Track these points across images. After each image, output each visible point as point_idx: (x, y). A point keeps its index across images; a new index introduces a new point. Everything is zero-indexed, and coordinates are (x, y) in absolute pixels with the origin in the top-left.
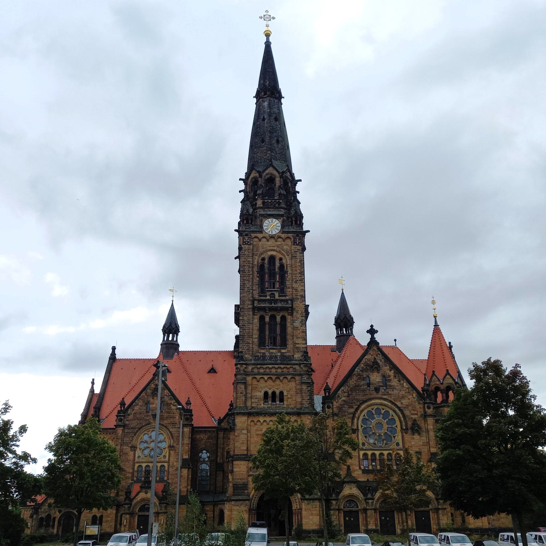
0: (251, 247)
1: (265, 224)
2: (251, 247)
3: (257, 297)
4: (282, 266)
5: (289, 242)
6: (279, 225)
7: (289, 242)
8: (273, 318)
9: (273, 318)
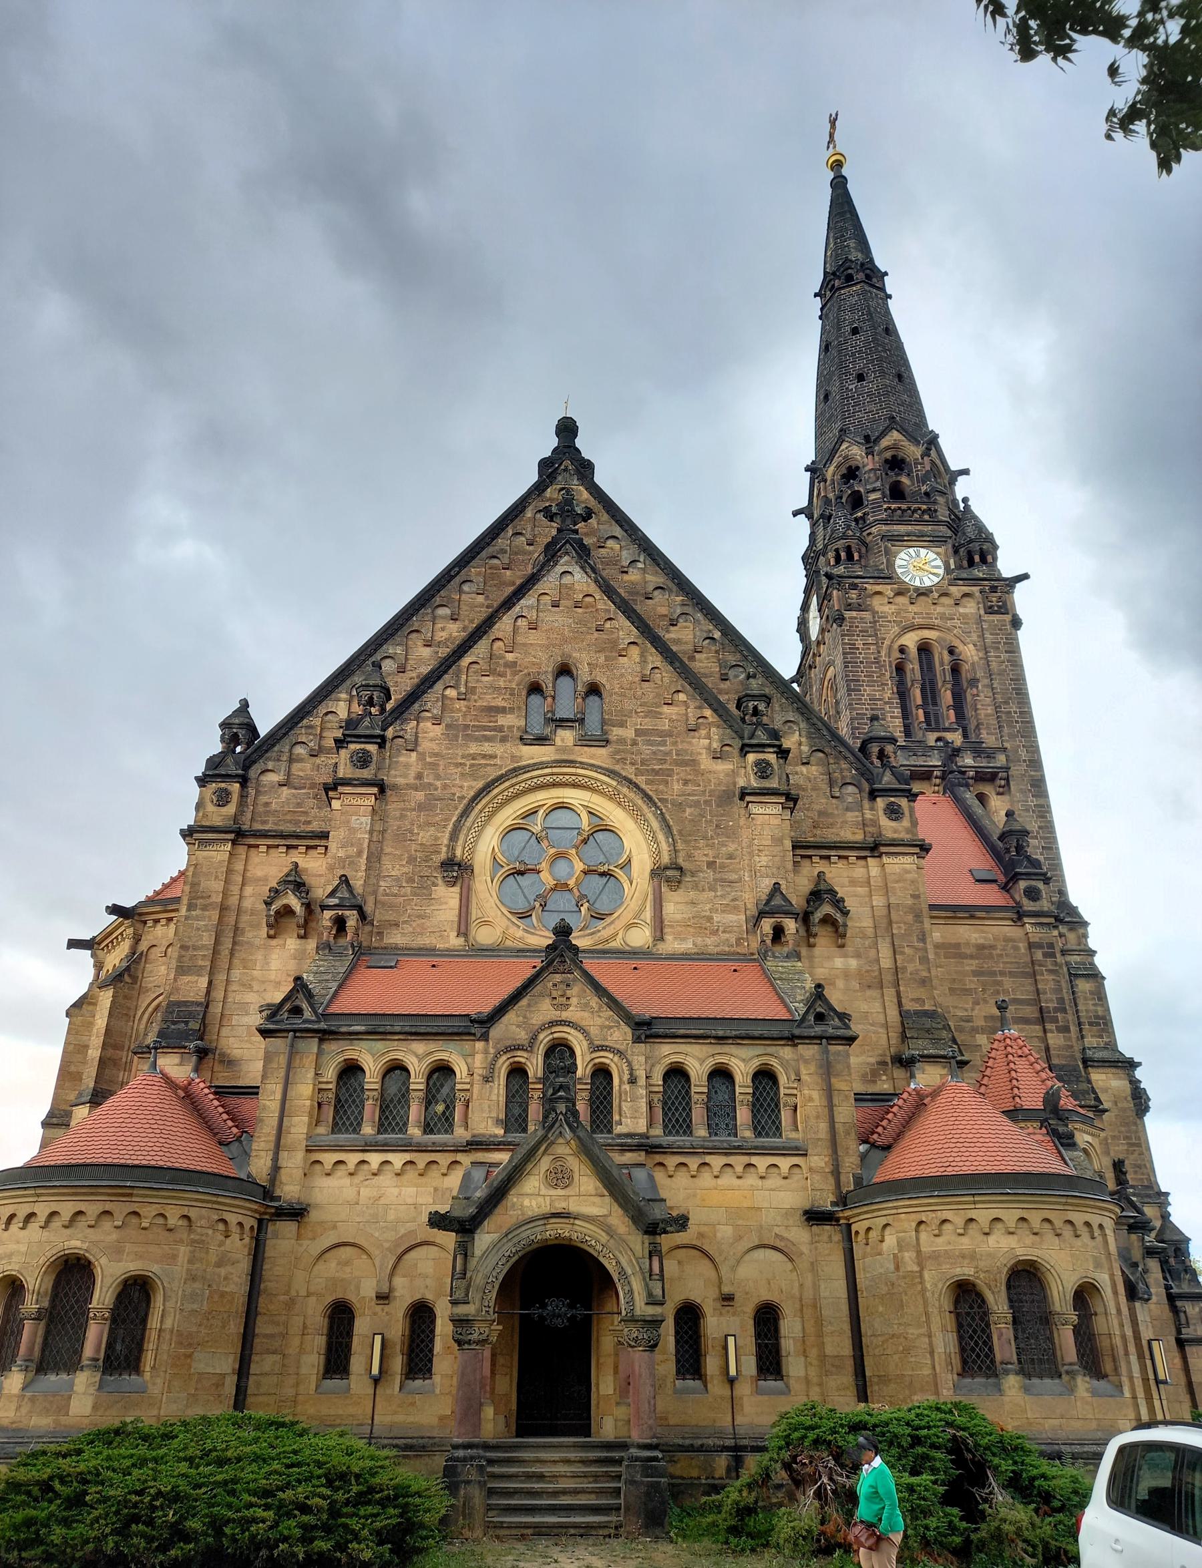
1: (898, 562)
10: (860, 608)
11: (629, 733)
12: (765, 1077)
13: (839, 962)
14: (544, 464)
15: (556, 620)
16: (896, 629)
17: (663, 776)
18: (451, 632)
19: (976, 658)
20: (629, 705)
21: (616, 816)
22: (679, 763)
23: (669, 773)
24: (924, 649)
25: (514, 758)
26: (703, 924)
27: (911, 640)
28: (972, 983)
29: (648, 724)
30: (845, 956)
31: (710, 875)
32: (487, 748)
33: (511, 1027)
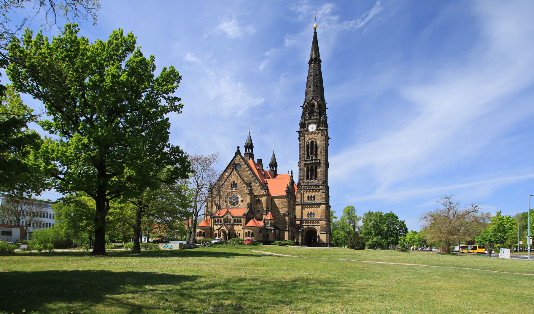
0: (303, 138)
2: (303, 138)
3: (306, 159)
4: (316, 145)
5: (320, 134)
6: (315, 127)
7: (320, 134)
8: (312, 167)
9: (312, 167)
10: (302, 137)
11: (239, 188)
12: (241, 220)
14: (236, 153)
17: (241, 192)
20: (239, 185)
21: (238, 196)
24: (312, 142)
26: (244, 205)
27: (310, 141)
28: (280, 204)
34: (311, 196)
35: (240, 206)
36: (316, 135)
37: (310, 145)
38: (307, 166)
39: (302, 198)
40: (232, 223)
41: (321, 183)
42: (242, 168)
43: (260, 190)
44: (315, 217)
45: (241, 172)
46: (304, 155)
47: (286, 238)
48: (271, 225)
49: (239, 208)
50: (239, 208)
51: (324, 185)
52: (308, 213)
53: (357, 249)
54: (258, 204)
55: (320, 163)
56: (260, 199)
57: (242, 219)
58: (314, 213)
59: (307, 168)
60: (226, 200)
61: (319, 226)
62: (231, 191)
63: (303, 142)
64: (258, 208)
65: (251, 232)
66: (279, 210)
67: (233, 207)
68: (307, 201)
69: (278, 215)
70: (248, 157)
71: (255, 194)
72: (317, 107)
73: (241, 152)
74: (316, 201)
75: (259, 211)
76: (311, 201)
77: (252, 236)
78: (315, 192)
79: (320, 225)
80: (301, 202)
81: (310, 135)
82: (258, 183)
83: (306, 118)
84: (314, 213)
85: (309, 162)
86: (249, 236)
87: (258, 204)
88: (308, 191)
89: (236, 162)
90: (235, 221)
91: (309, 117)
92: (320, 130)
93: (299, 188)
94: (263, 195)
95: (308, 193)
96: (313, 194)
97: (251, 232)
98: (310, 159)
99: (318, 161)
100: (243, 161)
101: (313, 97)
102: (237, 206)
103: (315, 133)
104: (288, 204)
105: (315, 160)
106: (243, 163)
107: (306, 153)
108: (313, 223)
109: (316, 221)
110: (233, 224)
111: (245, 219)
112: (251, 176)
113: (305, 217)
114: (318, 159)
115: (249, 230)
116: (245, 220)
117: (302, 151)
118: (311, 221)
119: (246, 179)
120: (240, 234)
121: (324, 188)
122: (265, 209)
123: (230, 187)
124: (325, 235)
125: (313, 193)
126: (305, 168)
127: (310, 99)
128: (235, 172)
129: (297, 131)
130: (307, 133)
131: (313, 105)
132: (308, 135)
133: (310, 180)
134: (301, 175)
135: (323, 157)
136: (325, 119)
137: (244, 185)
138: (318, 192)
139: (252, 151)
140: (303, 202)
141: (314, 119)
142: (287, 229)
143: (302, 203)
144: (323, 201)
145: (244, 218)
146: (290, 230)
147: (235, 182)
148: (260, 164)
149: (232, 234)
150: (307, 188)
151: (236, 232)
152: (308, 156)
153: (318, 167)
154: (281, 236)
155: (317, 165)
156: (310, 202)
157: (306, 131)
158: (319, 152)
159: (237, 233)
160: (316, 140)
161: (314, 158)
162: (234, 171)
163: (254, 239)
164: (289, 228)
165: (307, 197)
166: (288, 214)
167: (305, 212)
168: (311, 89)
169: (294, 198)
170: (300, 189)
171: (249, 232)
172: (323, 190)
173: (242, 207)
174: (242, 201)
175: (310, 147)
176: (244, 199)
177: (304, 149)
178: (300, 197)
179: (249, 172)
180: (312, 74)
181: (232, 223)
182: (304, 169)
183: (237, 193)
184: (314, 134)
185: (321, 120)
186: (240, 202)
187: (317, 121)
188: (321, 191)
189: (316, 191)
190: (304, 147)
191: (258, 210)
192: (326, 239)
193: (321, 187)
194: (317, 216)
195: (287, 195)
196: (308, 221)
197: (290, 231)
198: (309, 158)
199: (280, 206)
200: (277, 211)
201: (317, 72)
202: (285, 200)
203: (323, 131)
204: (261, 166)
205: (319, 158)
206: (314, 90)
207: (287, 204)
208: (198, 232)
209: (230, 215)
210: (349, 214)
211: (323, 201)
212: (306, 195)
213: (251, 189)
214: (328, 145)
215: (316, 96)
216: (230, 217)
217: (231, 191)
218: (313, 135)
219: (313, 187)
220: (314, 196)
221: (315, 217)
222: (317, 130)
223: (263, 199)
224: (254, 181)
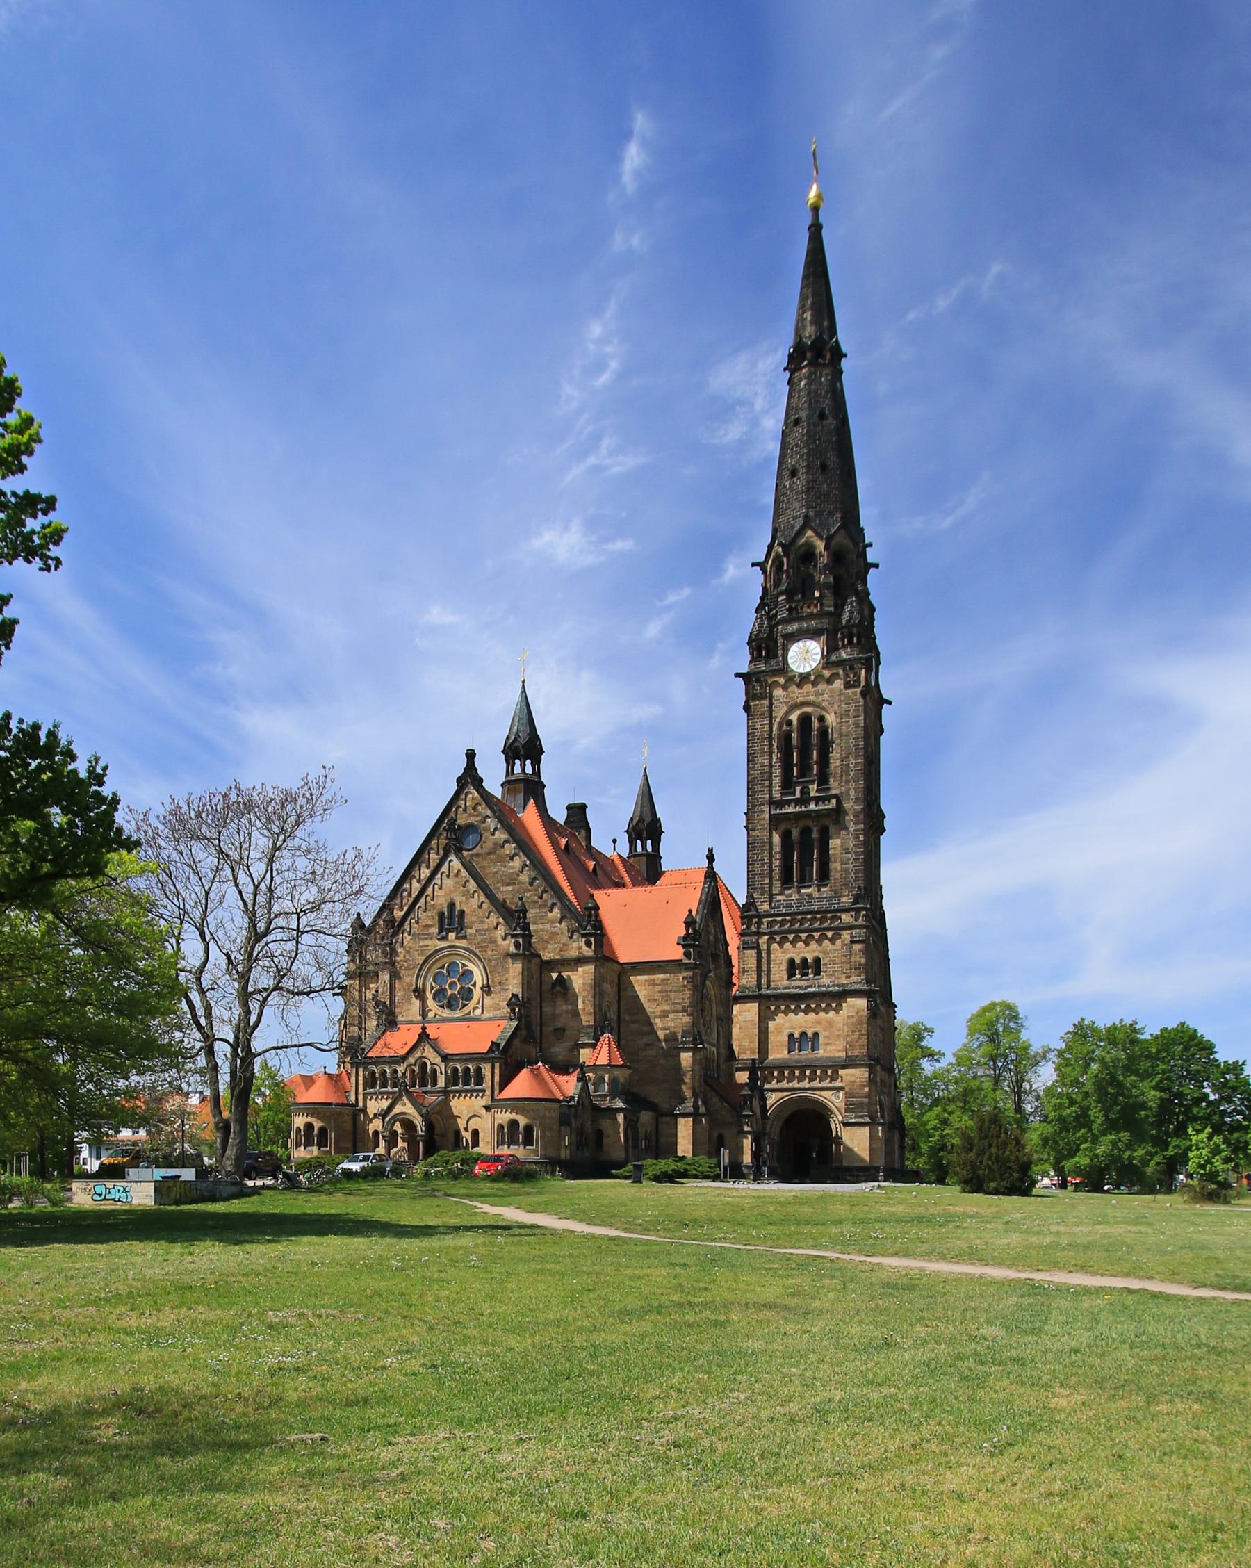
0: (766, 702)
2: (766, 702)
3: (777, 795)
4: (824, 731)
5: (838, 684)
6: (818, 650)
7: (838, 684)
8: (806, 832)
9: (806, 832)
10: (761, 697)
12: (479, 1070)
13: (564, 1007)
14: (459, 780)
15: (448, 883)
16: (785, 709)
18: (425, 873)
19: (834, 724)
20: (474, 919)
21: (471, 966)
22: (491, 942)
23: (487, 947)
24: (805, 720)
25: (435, 946)
27: (794, 717)
28: (657, 996)
29: (480, 926)
30: (566, 1004)
31: (499, 987)
32: (426, 942)
33: (411, 1060)
34: (804, 960)
35: (478, 1012)
36: (822, 687)
37: (795, 735)
38: (783, 827)
39: (764, 968)
40: (441, 1083)
41: (846, 900)
42: (488, 845)
43: (564, 939)
44: (821, 1053)
45: (484, 863)
46: (770, 779)
47: (684, 1145)
48: (613, 1094)
49: (477, 1019)
50: (477, 1019)
51: (858, 910)
52: (791, 1036)
53: (996, 1192)
54: (559, 1001)
55: (839, 811)
56: (565, 975)
57: (487, 1069)
58: (816, 1034)
59: (786, 837)
60: (420, 985)
61: (841, 1094)
62: (444, 944)
63: (766, 721)
64: (561, 1015)
65: (522, 1121)
66: (651, 1025)
67: (447, 1013)
68: (786, 983)
69: (648, 1045)
70: (521, 797)
71: (547, 956)
72: (823, 560)
73: (481, 773)
74: (825, 980)
75: (563, 1030)
76: (804, 983)
77: (528, 1141)
78: (819, 941)
79: (842, 1088)
80: (759, 987)
81: (793, 688)
82: (556, 910)
83: (775, 615)
84: (816, 1034)
85: (790, 809)
86: (512, 1141)
87: (559, 1001)
88: (791, 937)
89: (462, 819)
90: (453, 1078)
91: (790, 610)
92: (840, 663)
93: (748, 927)
94: (580, 961)
95: (787, 945)
96: (810, 952)
97: (522, 1121)
98: (798, 795)
99: (834, 801)
100: (489, 813)
101: (806, 517)
102: (466, 1010)
103: (819, 677)
104: (693, 996)
105: (817, 800)
106: (491, 823)
107: (777, 772)
108: (811, 1080)
109: (824, 1069)
110: (445, 1092)
111: (497, 1065)
112: (524, 878)
113: (778, 1053)
114: (833, 792)
115: (514, 1116)
116: (497, 1071)
117: (762, 760)
118: (803, 1069)
119: (505, 892)
120: (475, 1133)
121: (861, 921)
122: (587, 1020)
123: (435, 930)
124: (867, 1129)
125: (813, 945)
126: (776, 838)
127: (793, 527)
128: (456, 863)
129: (737, 675)
130: (782, 681)
131: (809, 555)
132: (785, 688)
133: (799, 888)
134: (758, 869)
135: (852, 785)
136: (861, 612)
137: (495, 918)
138: (832, 940)
139: (537, 773)
140: (768, 987)
141: (811, 617)
142: (689, 1106)
143: (764, 991)
144: (856, 981)
145: (492, 1061)
146: (702, 1110)
147: (458, 908)
148: (578, 828)
149: (443, 1136)
150: (782, 923)
151: (461, 1123)
152: (787, 784)
153: (832, 830)
154: (663, 1140)
155: (827, 822)
156: (799, 984)
157: (775, 672)
158: (838, 763)
159: (466, 1129)
160: (824, 709)
161: (813, 789)
162: (452, 857)
163: (535, 1152)
164: (696, 1102)
165: (784, 966)
166: (694, 1041)
167: (779, 1031)
168: (800, 483)
169: (724, 970)
170: (753, 929)
171: (514, 1124)
172: (854, 932)
173: (486, 1015)
174: (487, 989)
175: (795, 742)
176: (497, 981)
177: (771, 753)
178: (754, 966)
179: (517, 863)
180: (803, 415)
181: (441, 1083)
182: (771, 843)
183: (466, 953)
184: (814, 684)
185: (845, 617)
186: (477, 992)
187: (825, 623)
188: (846, 935)
189: (827, 938)
190: (771, 745)
191: (560, 1025)
192: (871, 1149)
193: (846, 918)
194: (831, 1049)
195: (687, 955)
196: (792, 1069)
197: (703, 1115)
198: (794, 794)
199: (659, 1009)
200: (646, 1029)
201: (826, 404)
202: (679, 978)
203: (852, 668)
204: (583, 833)
205: (835, 787)
206: (809, 489)
207: (686, 996)
208: (299, 1129)
209: (436, 1050)
210: (993, 1038)
211: (854, 979)
212: (781, 955)
213: (523, 936)
214: (882, 731)
215: (819, 514)
216: (431, 1057)
217: (444, 944)
218: (808, 687)
219: (813, 920)
220: (817, 961)
221: (821, 1053)
222: (827, 663)
223: (580, 979)
224: (541, 897)
